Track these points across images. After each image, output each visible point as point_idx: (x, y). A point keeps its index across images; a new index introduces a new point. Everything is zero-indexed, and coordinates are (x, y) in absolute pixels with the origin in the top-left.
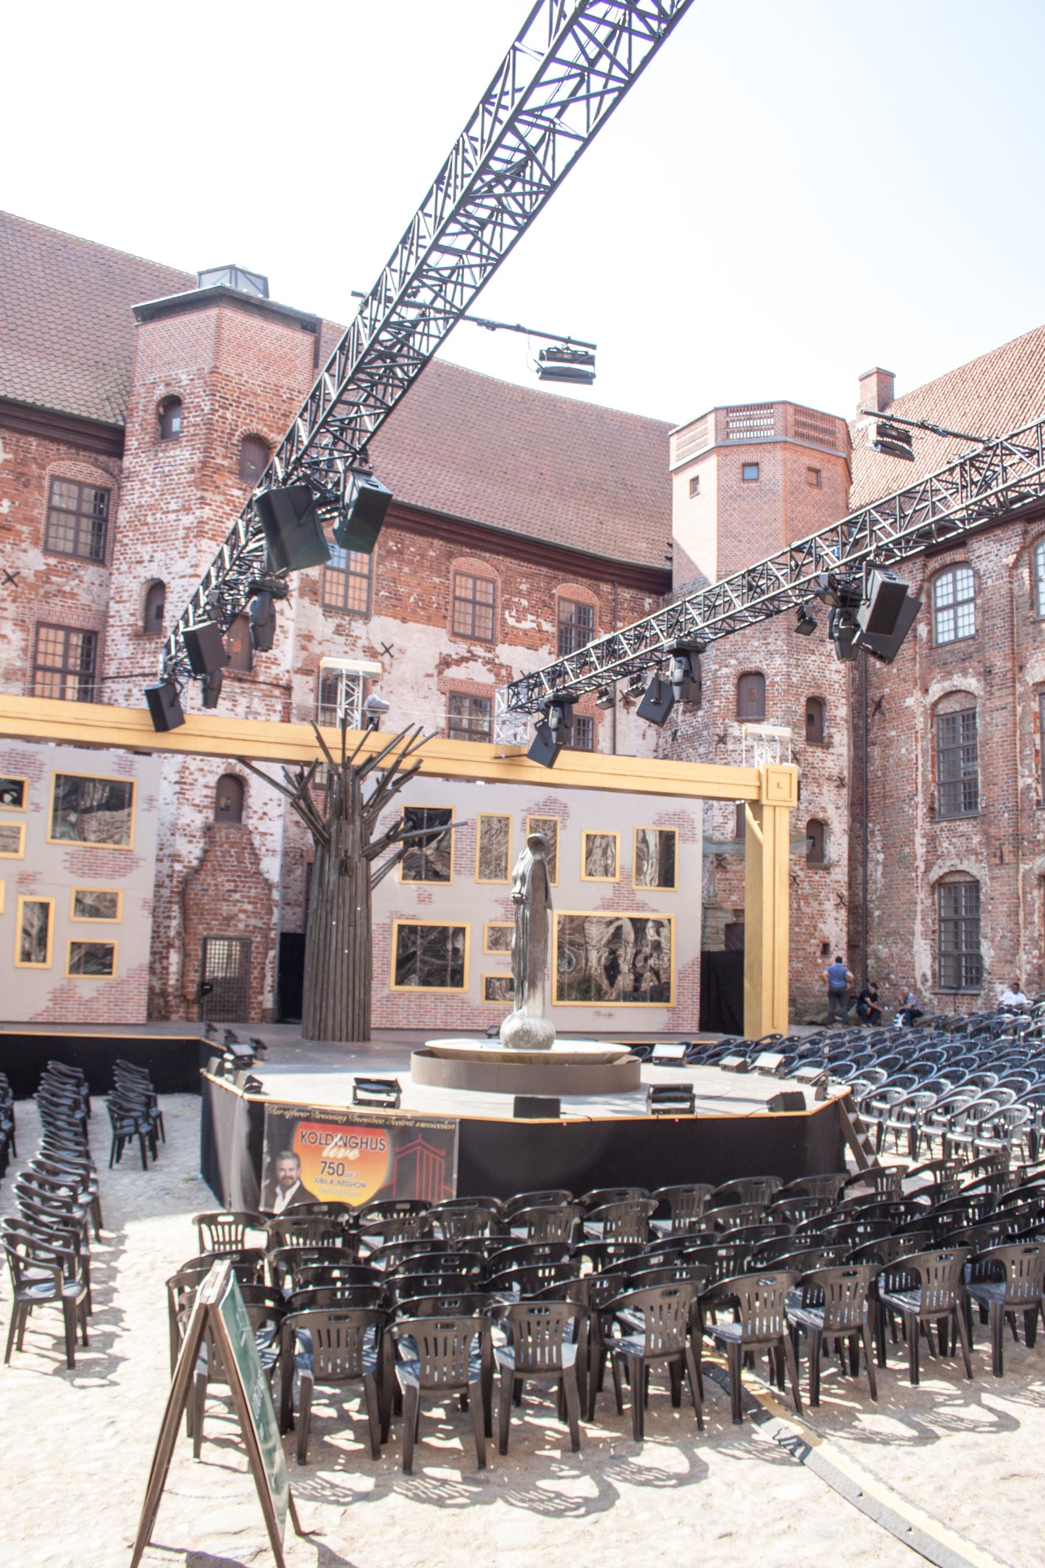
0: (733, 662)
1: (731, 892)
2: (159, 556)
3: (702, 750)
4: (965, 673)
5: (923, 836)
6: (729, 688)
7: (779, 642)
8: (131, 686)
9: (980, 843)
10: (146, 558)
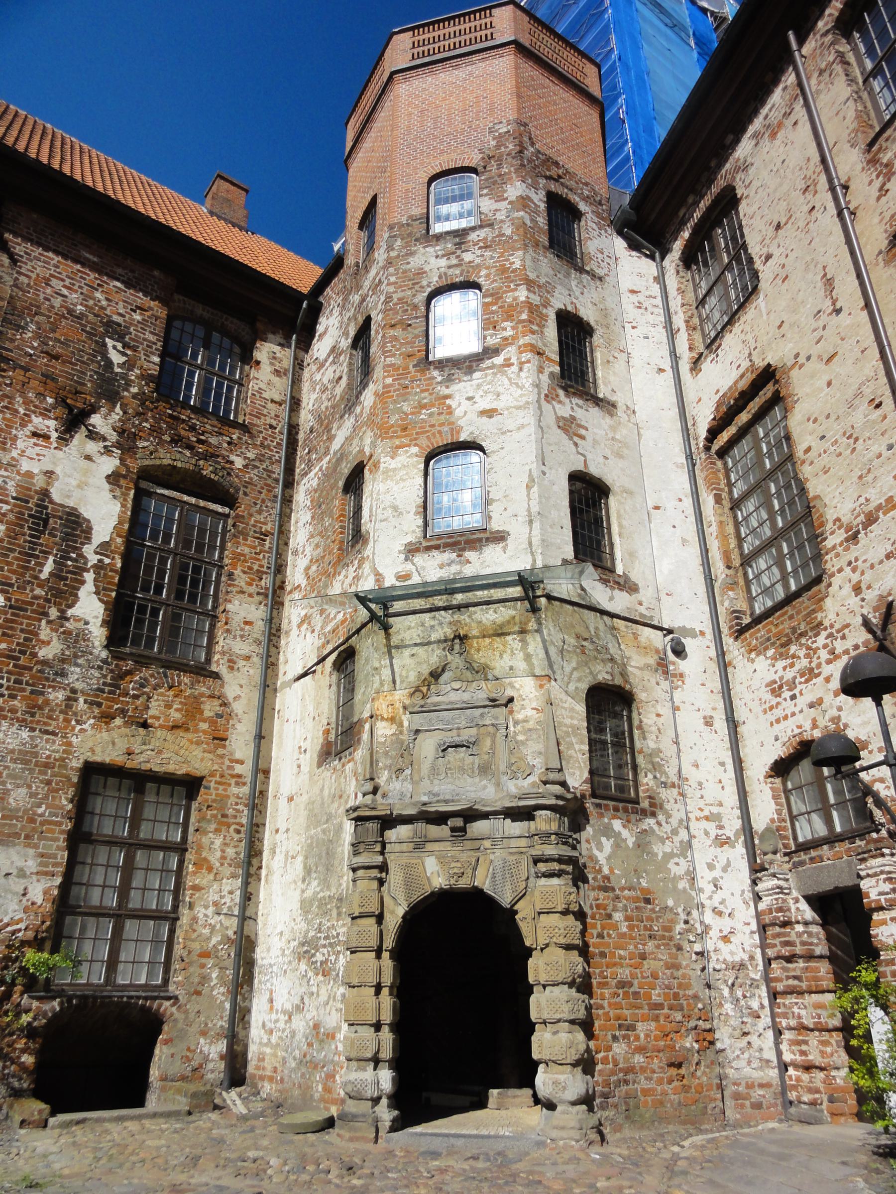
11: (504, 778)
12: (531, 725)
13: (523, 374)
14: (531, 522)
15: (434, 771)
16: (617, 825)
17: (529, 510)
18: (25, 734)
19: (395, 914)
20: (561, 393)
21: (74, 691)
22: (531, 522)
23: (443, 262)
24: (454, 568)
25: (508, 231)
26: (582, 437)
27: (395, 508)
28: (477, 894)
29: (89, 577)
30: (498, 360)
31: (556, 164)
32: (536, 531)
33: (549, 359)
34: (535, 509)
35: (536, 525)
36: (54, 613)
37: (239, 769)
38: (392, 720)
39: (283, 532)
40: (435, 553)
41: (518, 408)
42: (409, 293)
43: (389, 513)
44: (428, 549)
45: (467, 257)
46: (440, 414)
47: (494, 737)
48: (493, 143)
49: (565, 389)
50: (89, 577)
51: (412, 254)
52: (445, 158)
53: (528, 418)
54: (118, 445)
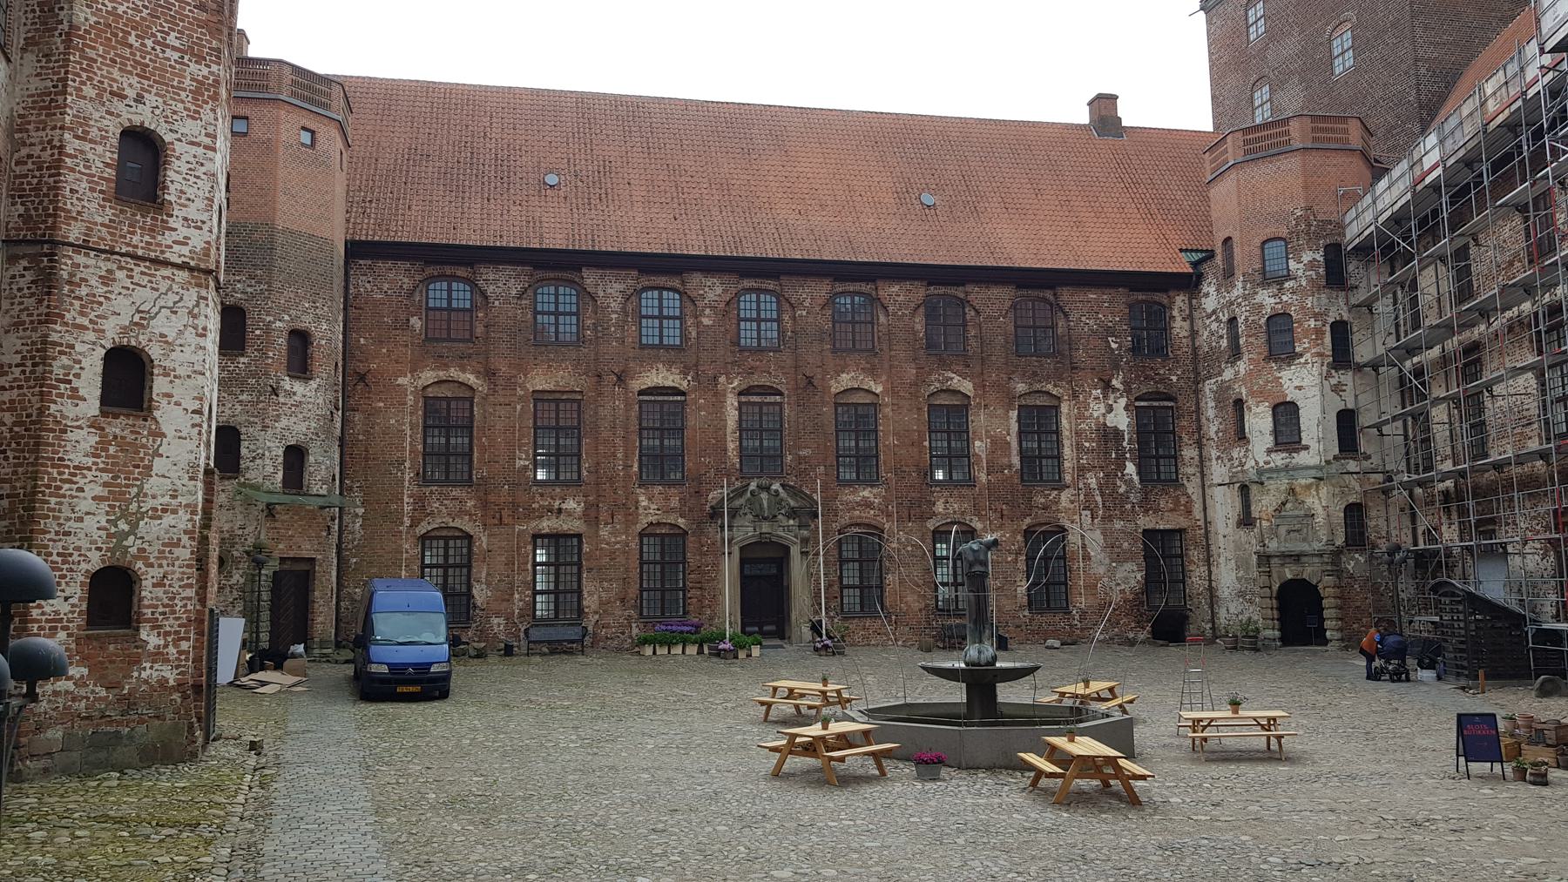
0: (287, 318)
1: (278, 541)
2: (151, 99)
3: (244, 397)
4: (463, 370)
5: (410, 497)
6: (282, 340)
7: (325, 308)
8: (110, 265)
9: (475, 506)
10: (131, 93)
15: (1286, 540)
16: (1357, 556)
19: (1276, 587)
20: (1333, 371)
23: (1273, 300)
24: (1288, 460)
25: (1304, 283)
26: (1344, 391)
30: (1302, 360)
31: (1330, 222)
32: (1321, 446)
34: (1321, 436)
36: (1120, 474)
37: (1198, 523)
39: (1198, 410)
42: (1257, 317)
43: (1258, 433)
44: (1276, 451)
45: (1285, 298)
48: (1294, 222)
51: (1256, 293)
52: (1268, 230)
53: (1316, 391)
54: (1125, 391)
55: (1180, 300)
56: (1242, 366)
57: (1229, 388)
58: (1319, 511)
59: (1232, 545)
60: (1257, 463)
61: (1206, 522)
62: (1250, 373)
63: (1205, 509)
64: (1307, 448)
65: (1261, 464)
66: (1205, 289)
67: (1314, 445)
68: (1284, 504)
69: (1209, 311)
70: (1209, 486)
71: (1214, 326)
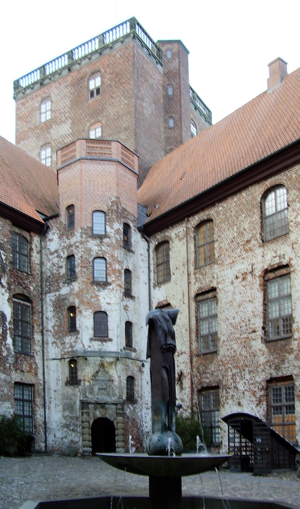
11: (112, 397)
12: (117, 386)
13: (117, 294)
14: (118, 338)
15: (98, 394)
17: (117, 334)
18: (4, 376)
19: (91, 422)
20: (124, 298)
21: (10, 364)
22: (118, 338)
24: (101, 347)
27: (87, 327)
28: (107, 418)
29: (8, 332)
32: (119, 340)
33: (122, 288)
35: (119, 339)
36: (4, 343)
38: (89, 382)
40: (97, 341)
41: (115, 304)
43: (85, 328)
44: (95, 340)
46: (97, 301)
47: (109, 388)
49: (125, 296)
50: (8, 332)
55: (36, 239)
56: (76, 286)
57: (65, 299)
58: (116, 378)
59: (60, 397)
60: (84, 346)
61: (44, 382)
62: (81, 291)
63: (44, 374)
64: (111, 340)
65: (86, 347)
66: (50, 235)
67: (115, 339)
68: (97, 372)
69: (53, 250)
70: (47, 359)
71: (56, 260)
